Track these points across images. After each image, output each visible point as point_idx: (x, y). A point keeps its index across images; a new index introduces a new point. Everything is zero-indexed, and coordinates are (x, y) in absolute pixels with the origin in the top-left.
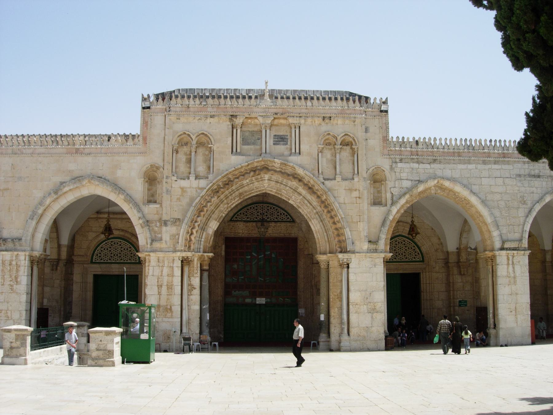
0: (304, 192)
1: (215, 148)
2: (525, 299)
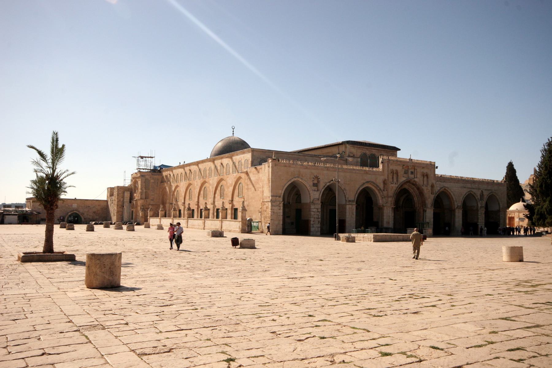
0: (415, 189)
1: (399, 174)
2: (461, 222)
